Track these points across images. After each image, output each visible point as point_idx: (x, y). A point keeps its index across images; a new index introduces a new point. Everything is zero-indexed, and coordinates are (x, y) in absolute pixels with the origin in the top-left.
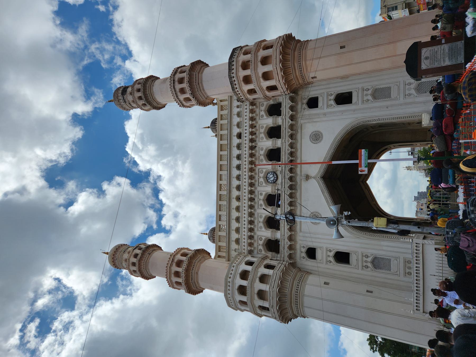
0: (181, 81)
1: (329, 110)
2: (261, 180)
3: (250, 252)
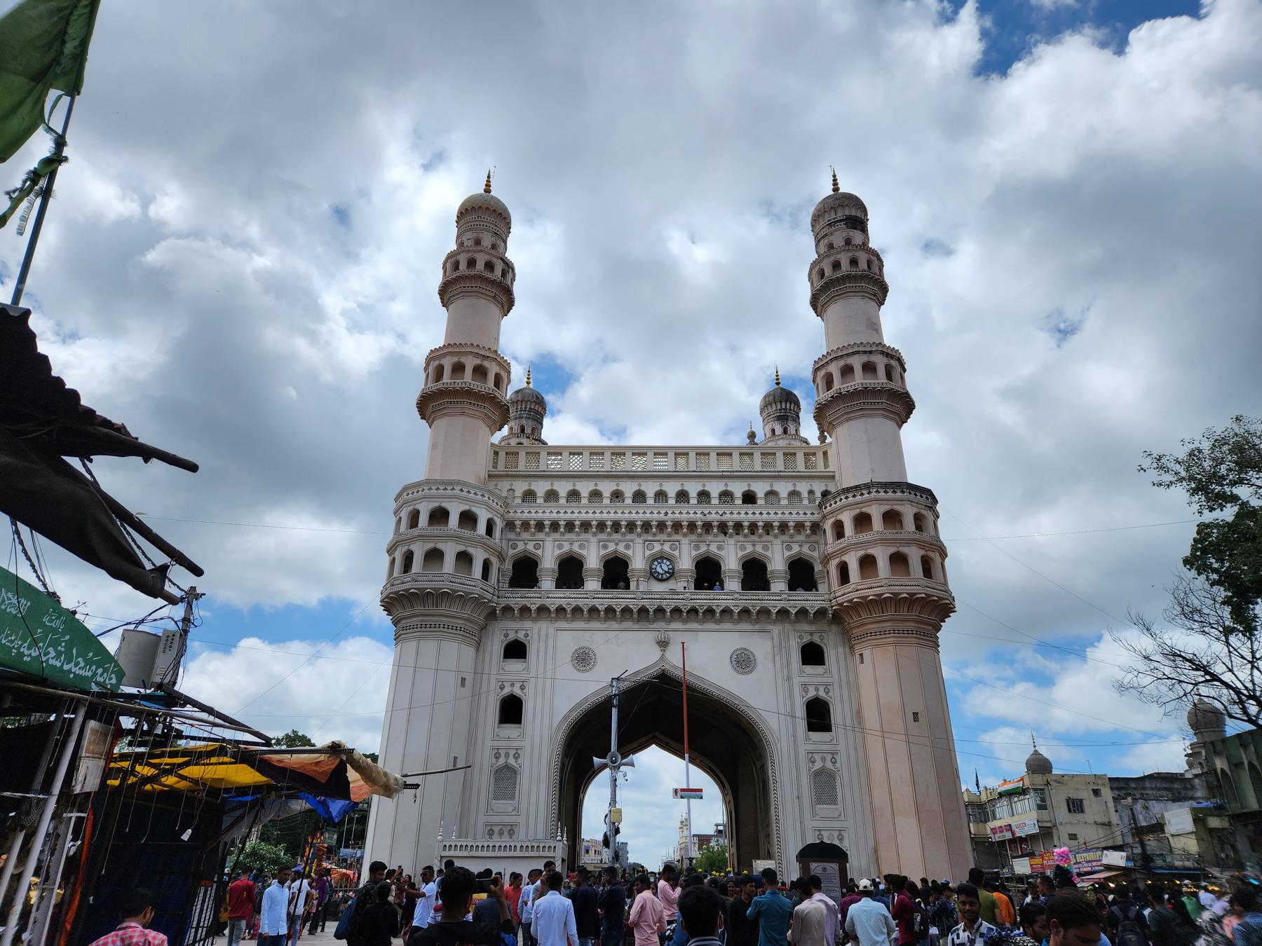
2: (657, 547)
3: (510, 525)
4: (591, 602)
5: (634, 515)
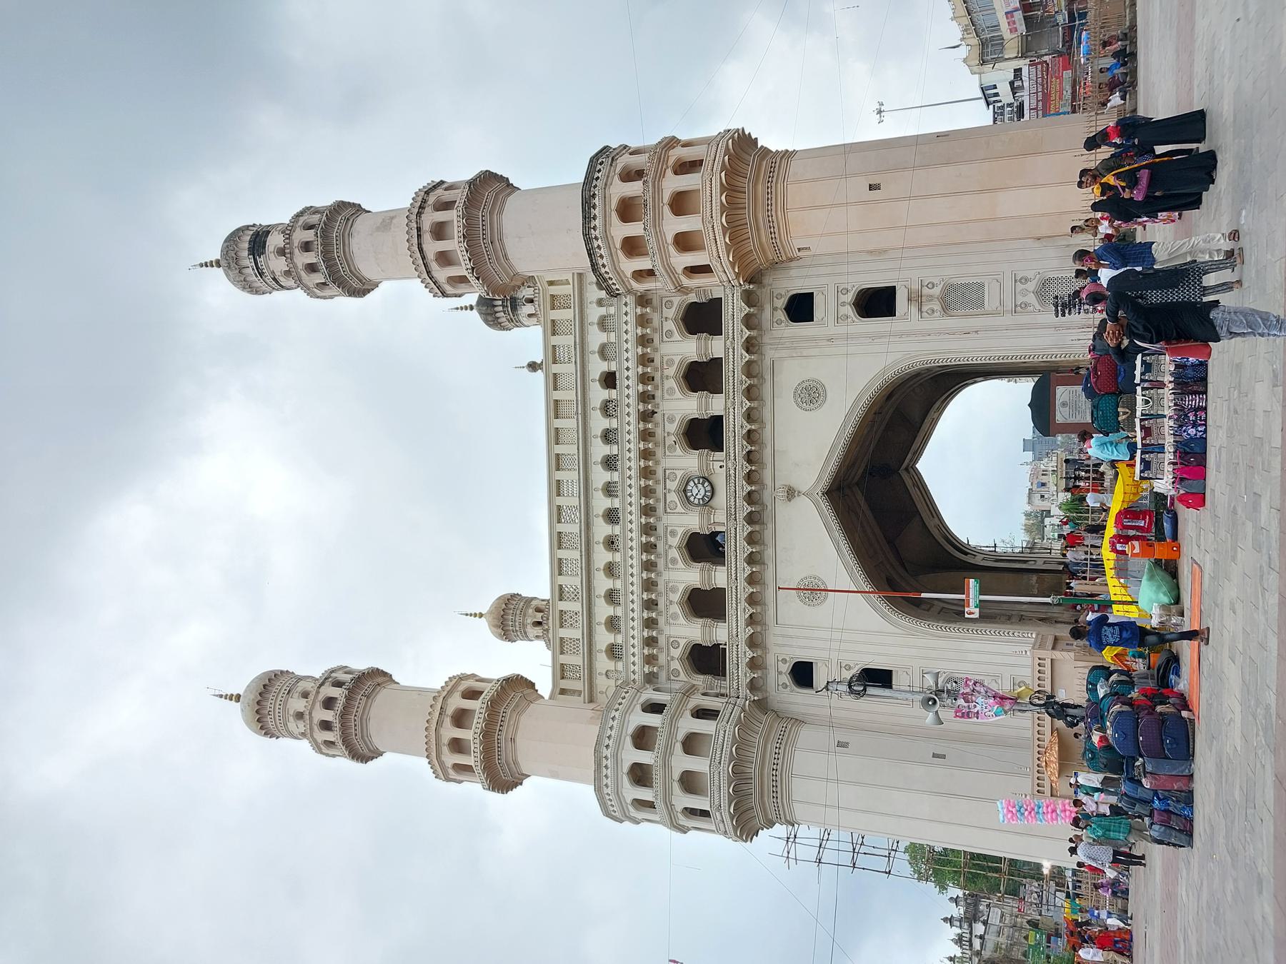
0: (440, 231)
1: (841, 329)
2: (673, 497)
4: (742, 583)
5: (634, 544)
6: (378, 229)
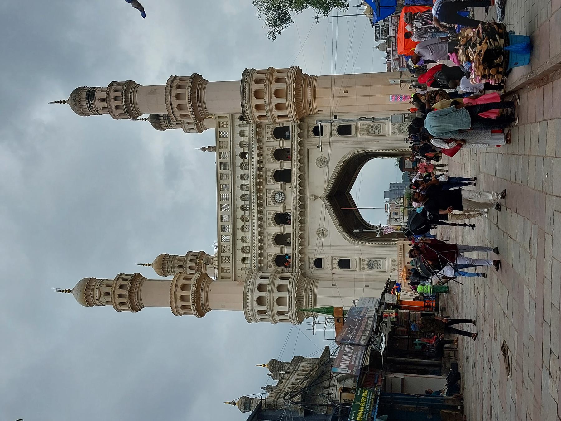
4: (297, 230)
6: (149, 94)
